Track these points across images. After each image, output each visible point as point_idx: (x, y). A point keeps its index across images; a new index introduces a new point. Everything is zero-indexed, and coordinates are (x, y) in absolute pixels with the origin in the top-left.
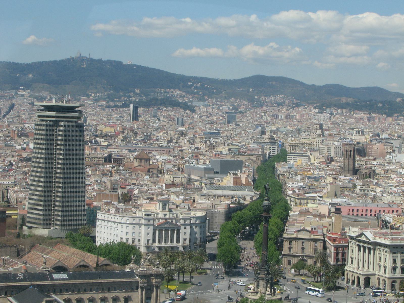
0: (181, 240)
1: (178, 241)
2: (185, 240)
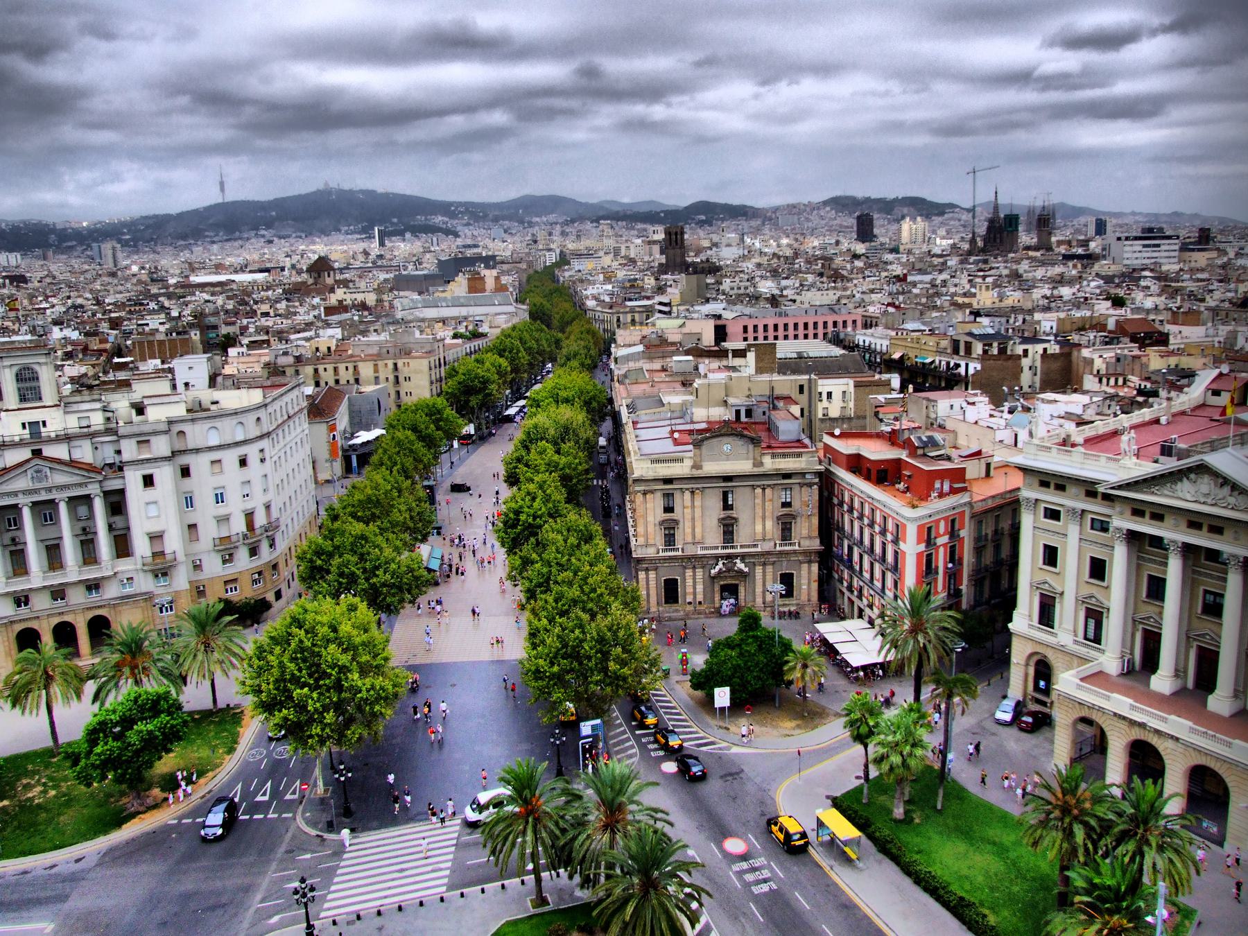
0: (141, 546)
1: (122, 547)
2: (156, 537)
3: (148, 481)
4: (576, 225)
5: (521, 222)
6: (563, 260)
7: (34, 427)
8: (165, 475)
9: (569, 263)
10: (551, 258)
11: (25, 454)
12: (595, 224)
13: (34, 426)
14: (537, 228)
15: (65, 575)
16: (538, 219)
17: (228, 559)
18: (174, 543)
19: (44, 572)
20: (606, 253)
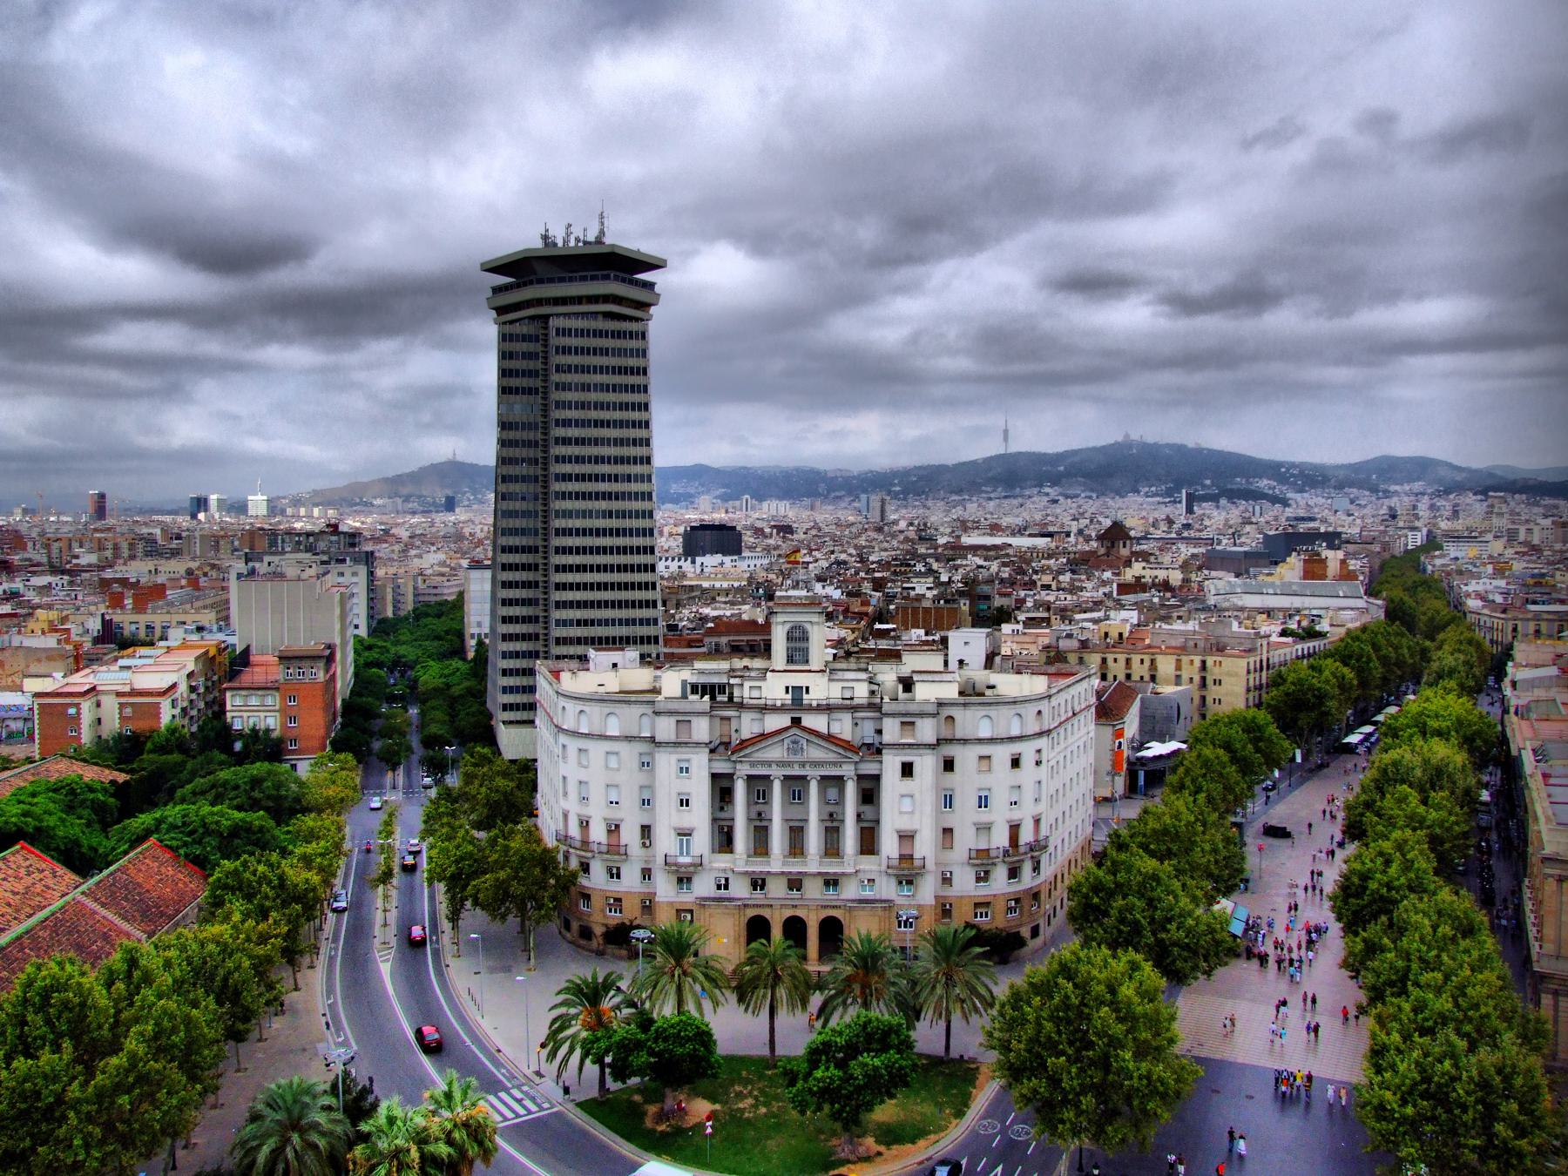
0: (889, 846)
1: (869, 843)
2: (906, 837)
3: (907, 770)
4: (1452, 497)
5: (1374, 490)
6: (1432, 544)
7: (797, 692)
8: (926, 765)
9: (1441, 548)
10: (1416, 539)
11: (784, 720)
12: (1479, 497)
13: (797, 692)
14: (1395, 499)
15: (768, 863)
16: (1397, 488)
17: (983, 877)
18: (925, 847)
19: (749, 856)
20: (1496, 537)
